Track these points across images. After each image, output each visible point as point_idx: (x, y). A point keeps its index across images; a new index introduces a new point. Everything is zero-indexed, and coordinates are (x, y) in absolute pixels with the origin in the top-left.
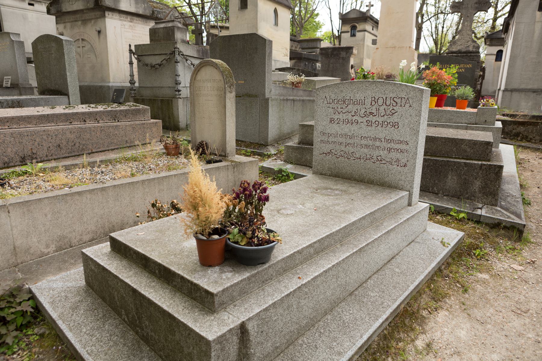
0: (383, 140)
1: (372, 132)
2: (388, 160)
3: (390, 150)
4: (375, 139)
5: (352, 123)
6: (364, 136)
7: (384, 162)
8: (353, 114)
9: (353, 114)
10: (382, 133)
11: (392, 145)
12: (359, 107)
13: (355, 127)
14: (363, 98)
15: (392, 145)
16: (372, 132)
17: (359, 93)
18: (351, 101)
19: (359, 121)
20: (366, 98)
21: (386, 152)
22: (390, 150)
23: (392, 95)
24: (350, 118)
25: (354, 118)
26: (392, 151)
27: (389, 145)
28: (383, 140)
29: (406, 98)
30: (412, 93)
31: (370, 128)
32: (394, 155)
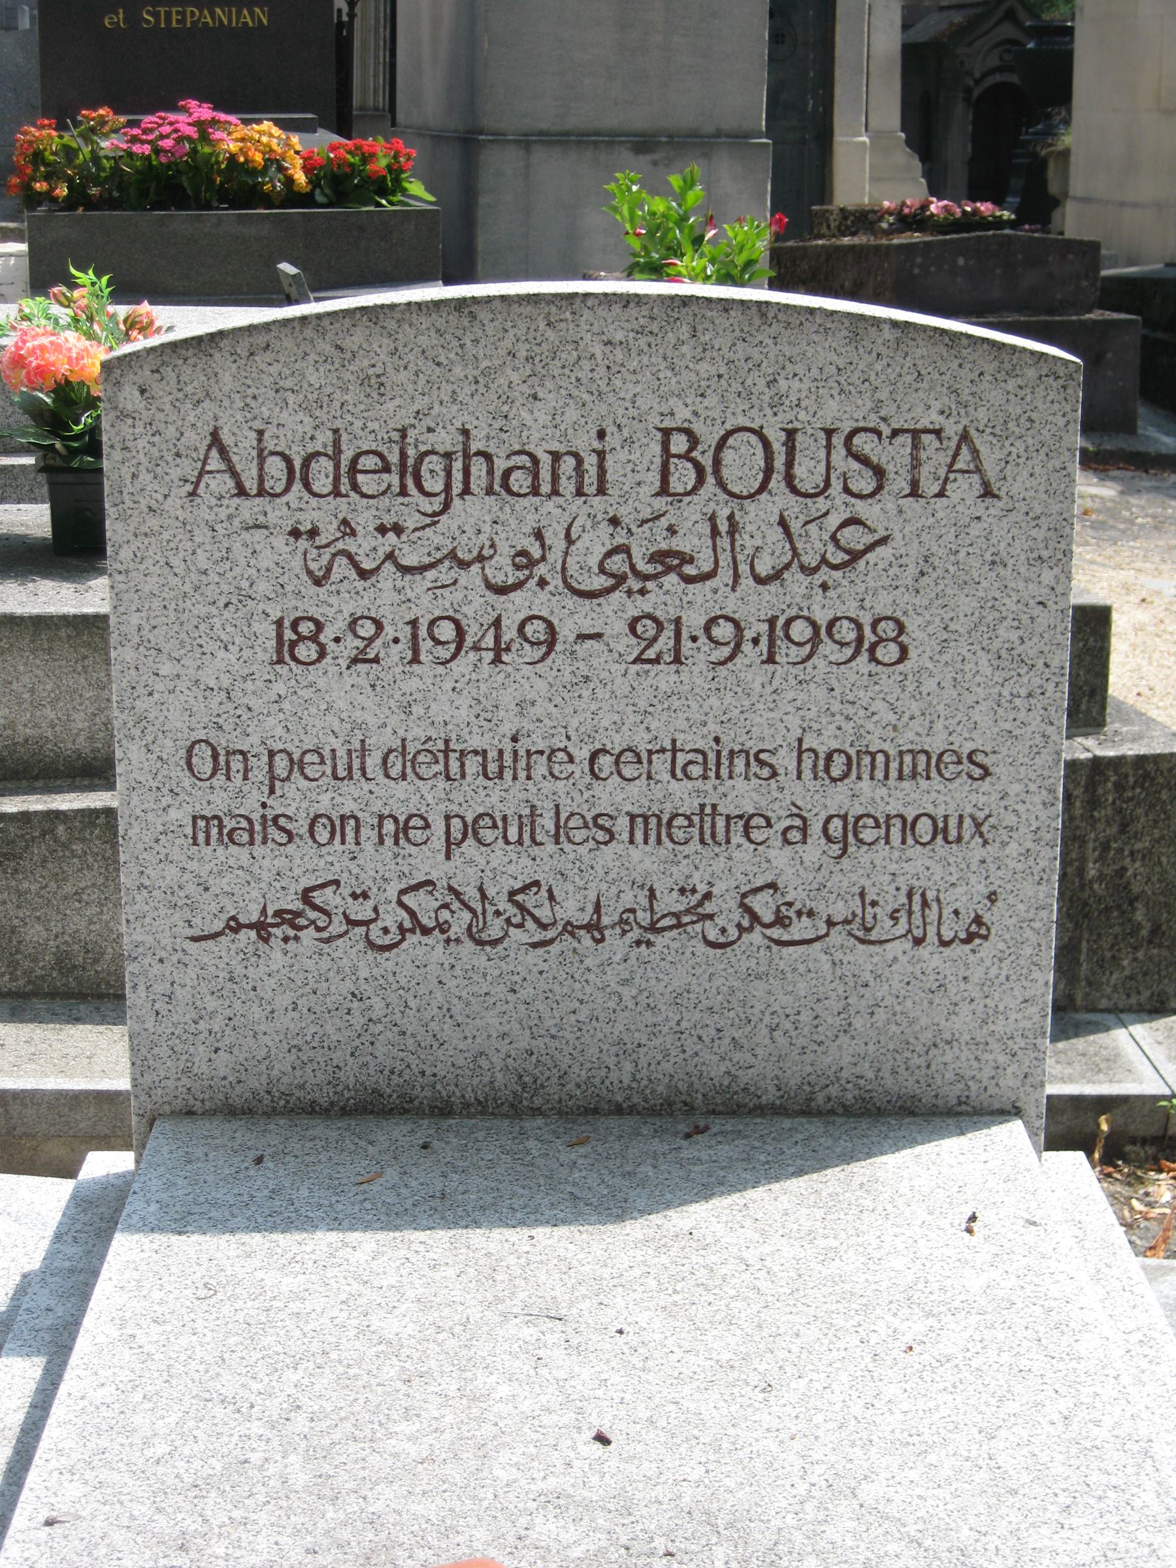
0: (785, 761)
1: (695, 702)
2: (839, 911)
3: (846, 834)
4: (716, 761)
5: (499, 651)
6: (617, 743)
7: (801, 929)
8: (502, 570)
9: (502, 570)
10: (774, 705)
11: (868, 795)
12: (551, 515)
13: (525, 679)
14: (584, 442)
15: (868, 795)
16: (695, 702)
17: (551, 400)
18: (478, 468)
19: (566, 632)
20: (613, 440)
21: (815, 850)
22: (846, 834)
23: (838, 412)
24: (476, 606)
25: (515, 607)
26: (868, 835)
27: (838, 798)
28: (785, 761)
29: (952, 429)
30: (995, 396)
31: (664, 677)
32: (884, 869)
